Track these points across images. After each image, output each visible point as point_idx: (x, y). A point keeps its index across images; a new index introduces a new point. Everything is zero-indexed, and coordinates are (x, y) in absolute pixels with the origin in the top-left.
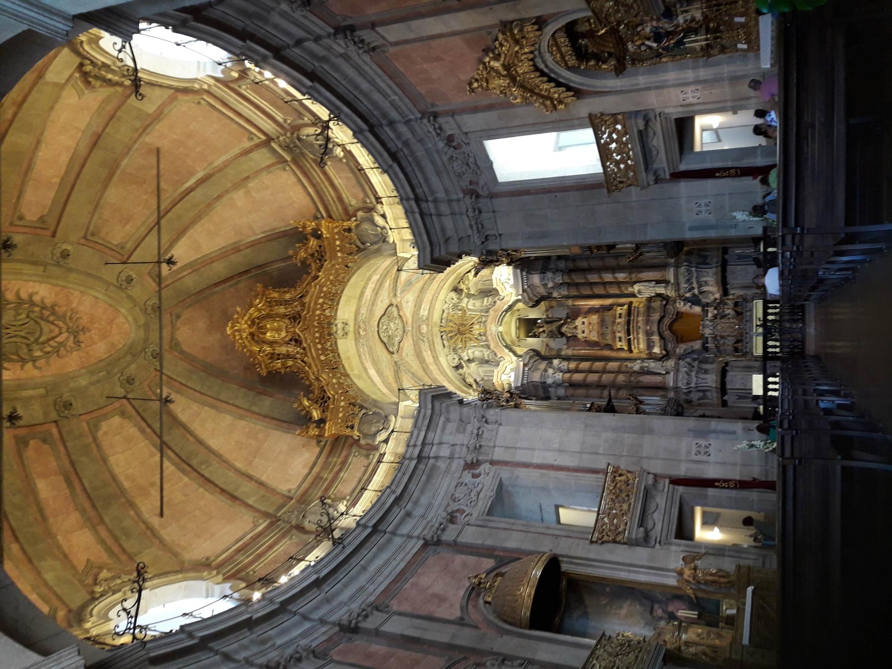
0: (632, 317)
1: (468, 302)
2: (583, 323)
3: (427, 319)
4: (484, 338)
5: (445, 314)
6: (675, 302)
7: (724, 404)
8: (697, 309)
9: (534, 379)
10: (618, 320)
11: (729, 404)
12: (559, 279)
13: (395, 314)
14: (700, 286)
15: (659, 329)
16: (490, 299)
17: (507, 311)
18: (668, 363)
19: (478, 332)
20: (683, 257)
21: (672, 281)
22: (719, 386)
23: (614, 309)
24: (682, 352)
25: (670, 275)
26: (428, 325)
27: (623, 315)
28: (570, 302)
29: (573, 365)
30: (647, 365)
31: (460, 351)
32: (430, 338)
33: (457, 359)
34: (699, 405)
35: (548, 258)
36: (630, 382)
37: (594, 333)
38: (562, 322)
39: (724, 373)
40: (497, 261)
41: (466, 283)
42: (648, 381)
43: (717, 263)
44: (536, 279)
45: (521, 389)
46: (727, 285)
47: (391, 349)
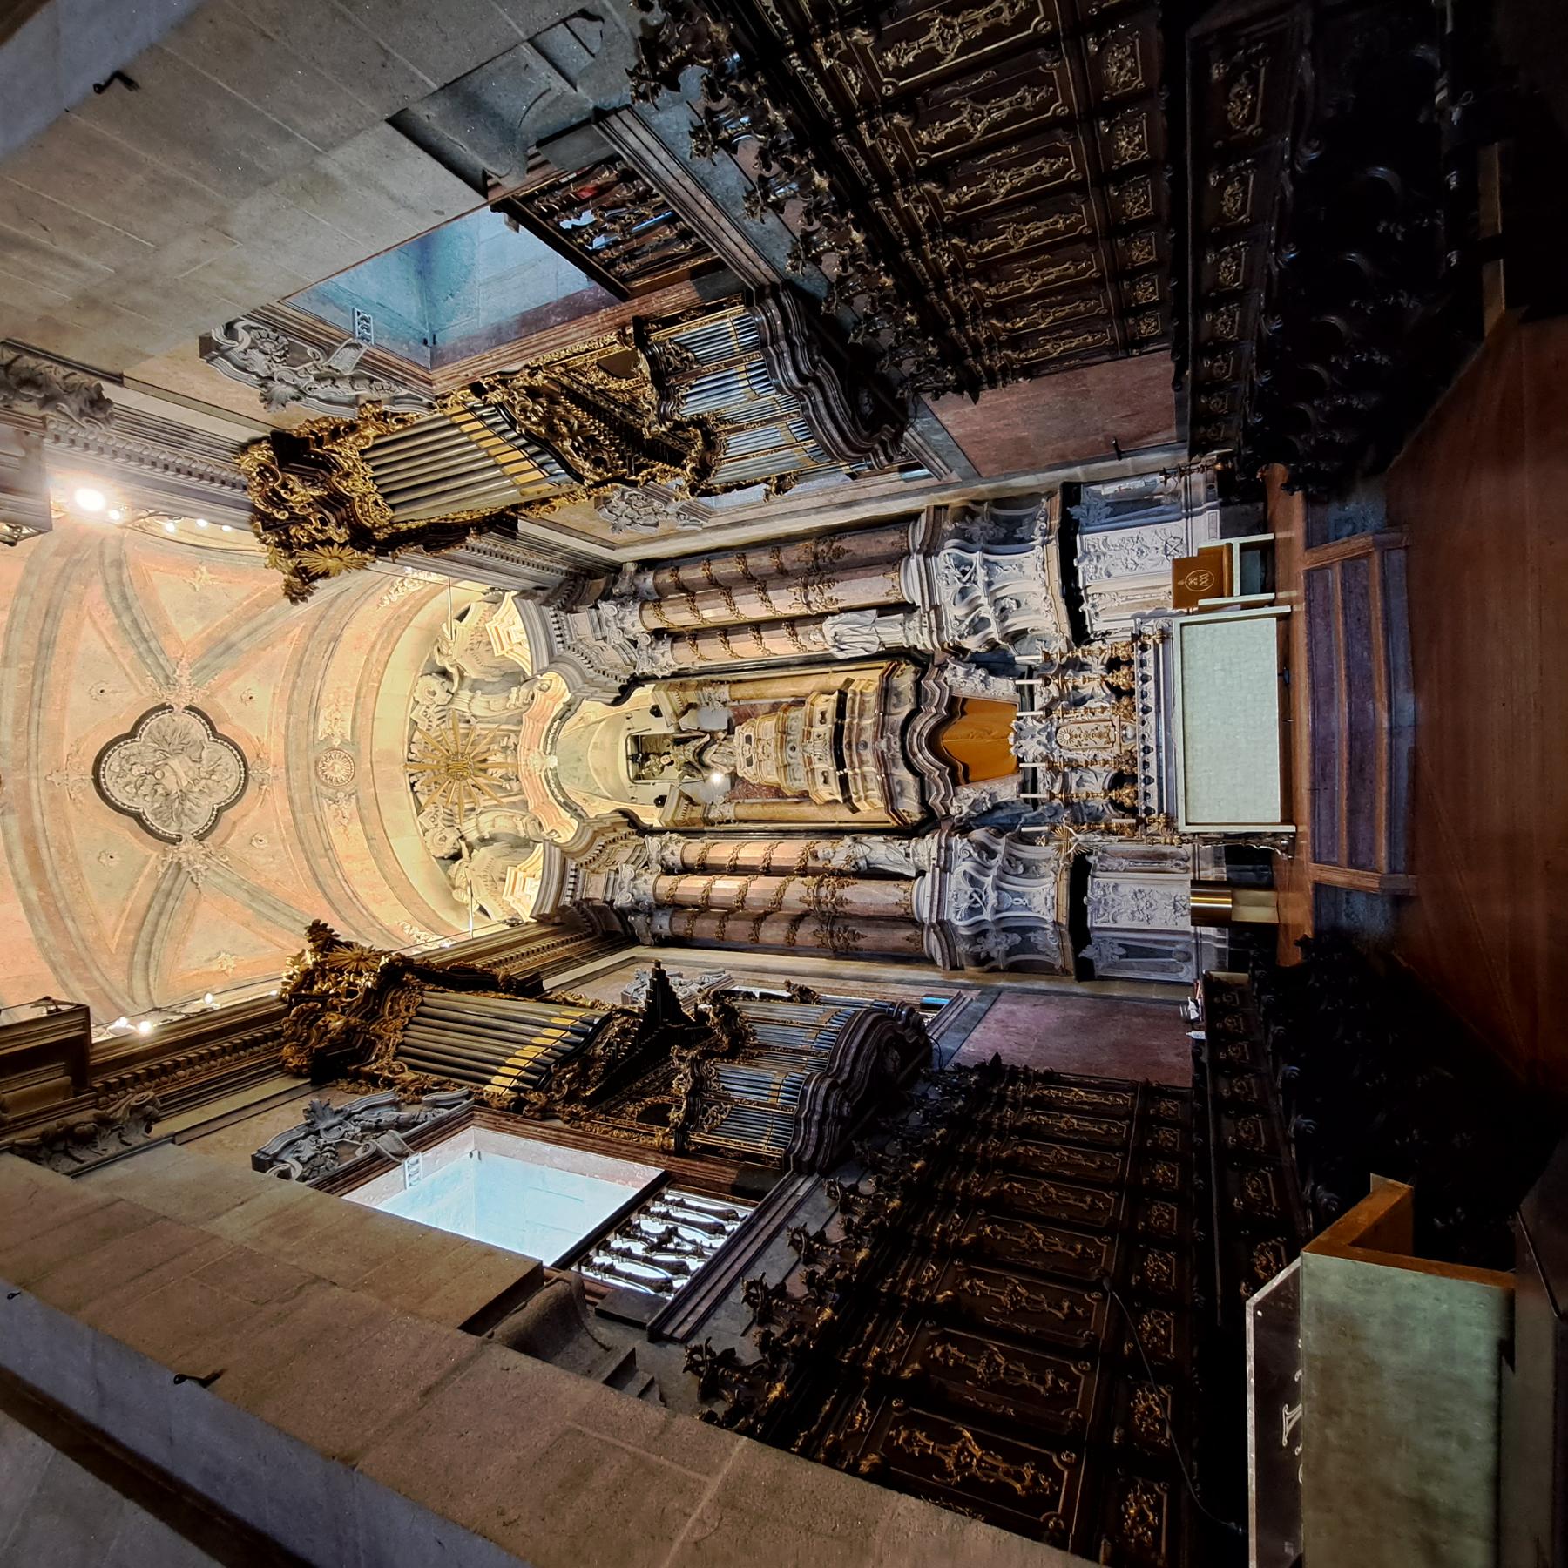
0: (848, 720)
1: (473, 697)
2: (748, 739)
3: (354, 742)
4: (514, 784)
5: (417, 733)
6: (942, 667)
7: (1085, 971)
8: (1003, 687)
9: (590, 895)
10: (819, 729)
11: (1099, 972)
12: (638, 621)
13: (198, 730)
14: (1003, 613)
15: (903, 747)
16: (524, 689)
17: (563, 717)
18: (920, 847)
19: (501, 772)
20: (948, 527)
21: (918, 603)
22: (1064, 922)
23: (809, 700)
24: (965, 810)
25: (908, 582)
26: (353, 761)
27: (829, 716)
28: (724, 692)
29: (693, 850)
30: (867, 850)
31: (457, 821)
32: (366, 793)
33: (452, 837)
34: (1016, 969)
35: (616, 569)
36: (819, 903)
37: (769, 762)
38: (707, 738)
39: (1079, 872)
40: (329, 542)
41: (444, 649)
42: (868, 900)
43: (1047, 533)
44: (582, 621)
45: (557, 920)
46: (1081, 602)
47: (171, 831)
